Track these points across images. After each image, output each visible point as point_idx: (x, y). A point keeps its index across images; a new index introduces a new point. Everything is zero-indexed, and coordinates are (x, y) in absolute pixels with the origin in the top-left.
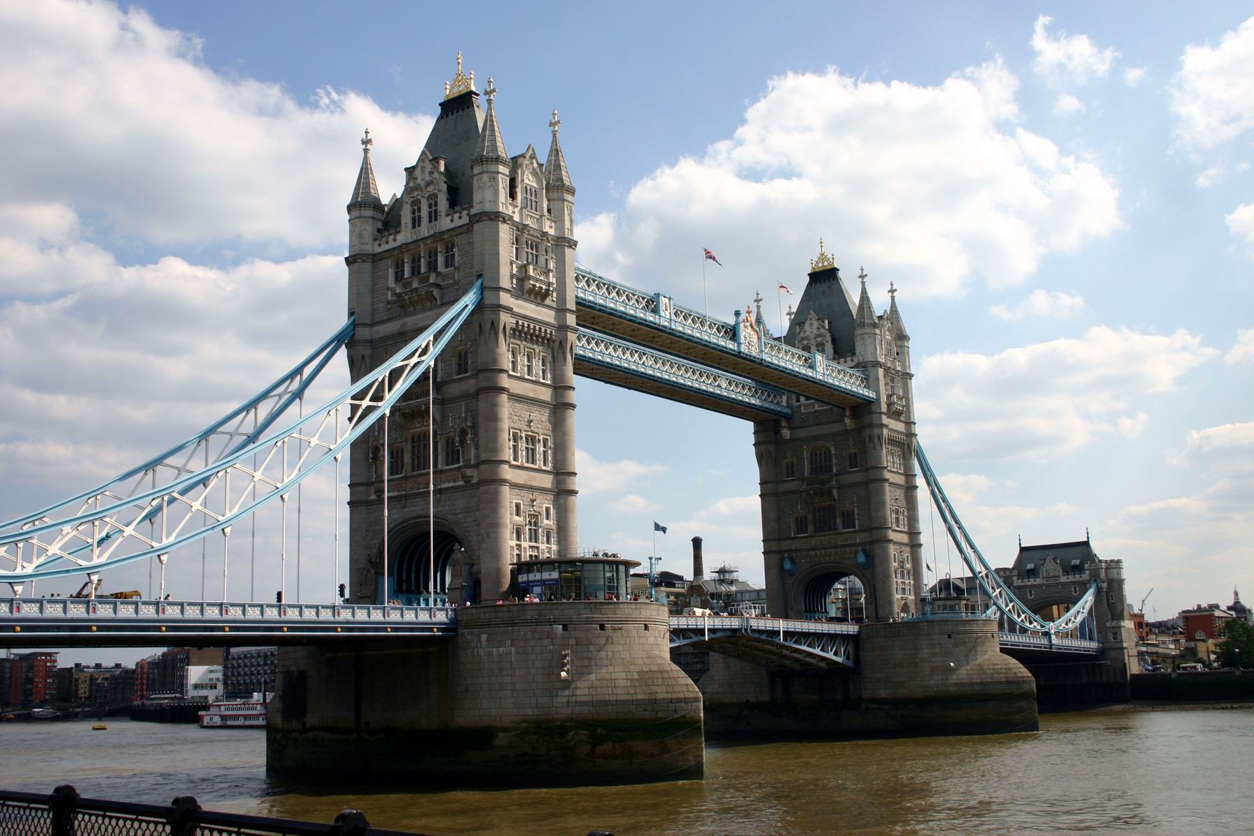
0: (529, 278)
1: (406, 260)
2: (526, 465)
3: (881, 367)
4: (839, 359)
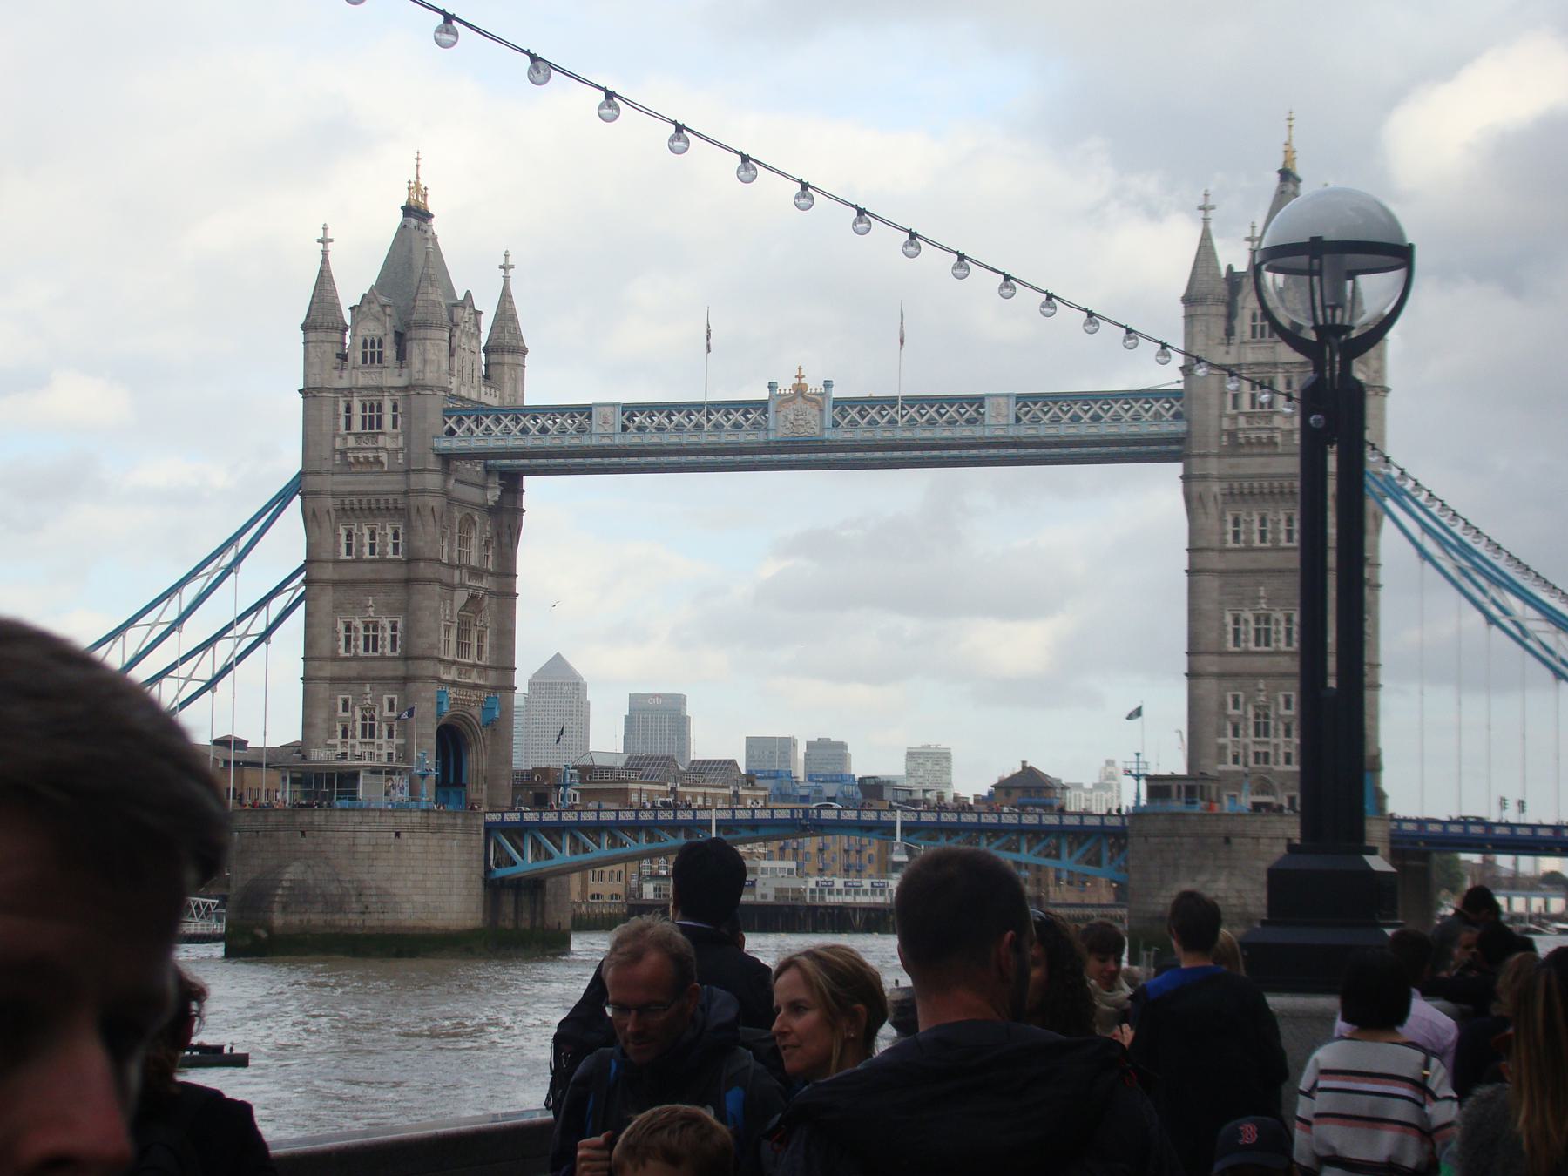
0: (349, 449)
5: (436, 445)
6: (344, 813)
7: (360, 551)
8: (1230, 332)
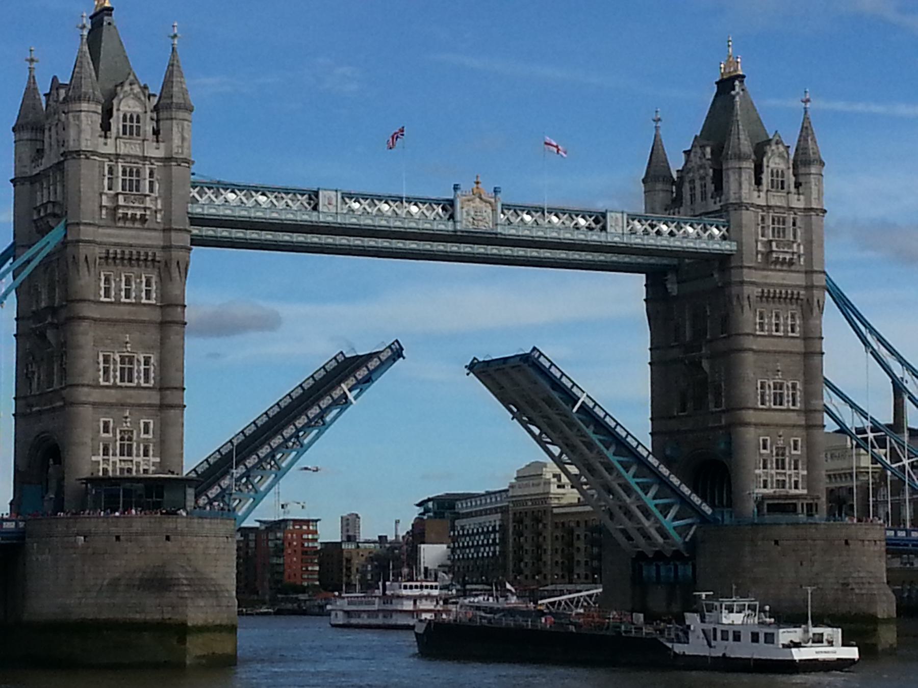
0: (118, 207)
1: (45, 186)
2: (119, 383)
3: (747, 209)
4: (715, 198)
5: (190, 210)
6: (200, 520)
7: (118, 295)
8: (758, 182)
